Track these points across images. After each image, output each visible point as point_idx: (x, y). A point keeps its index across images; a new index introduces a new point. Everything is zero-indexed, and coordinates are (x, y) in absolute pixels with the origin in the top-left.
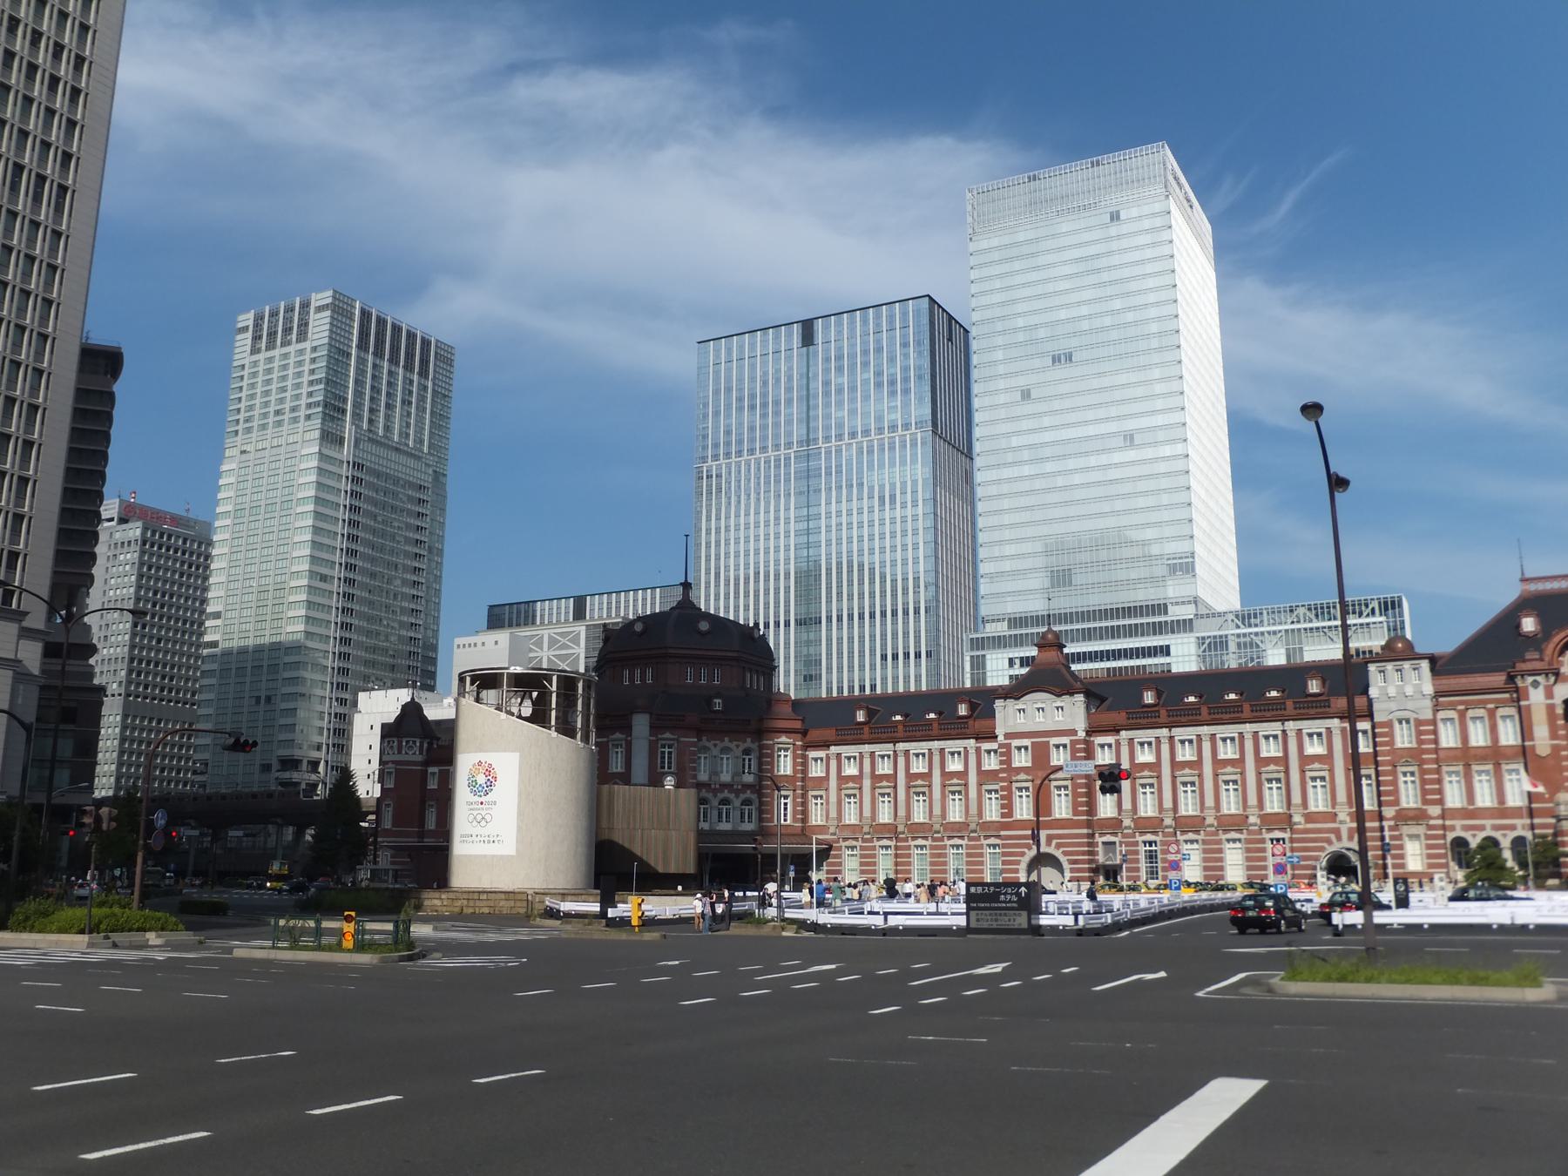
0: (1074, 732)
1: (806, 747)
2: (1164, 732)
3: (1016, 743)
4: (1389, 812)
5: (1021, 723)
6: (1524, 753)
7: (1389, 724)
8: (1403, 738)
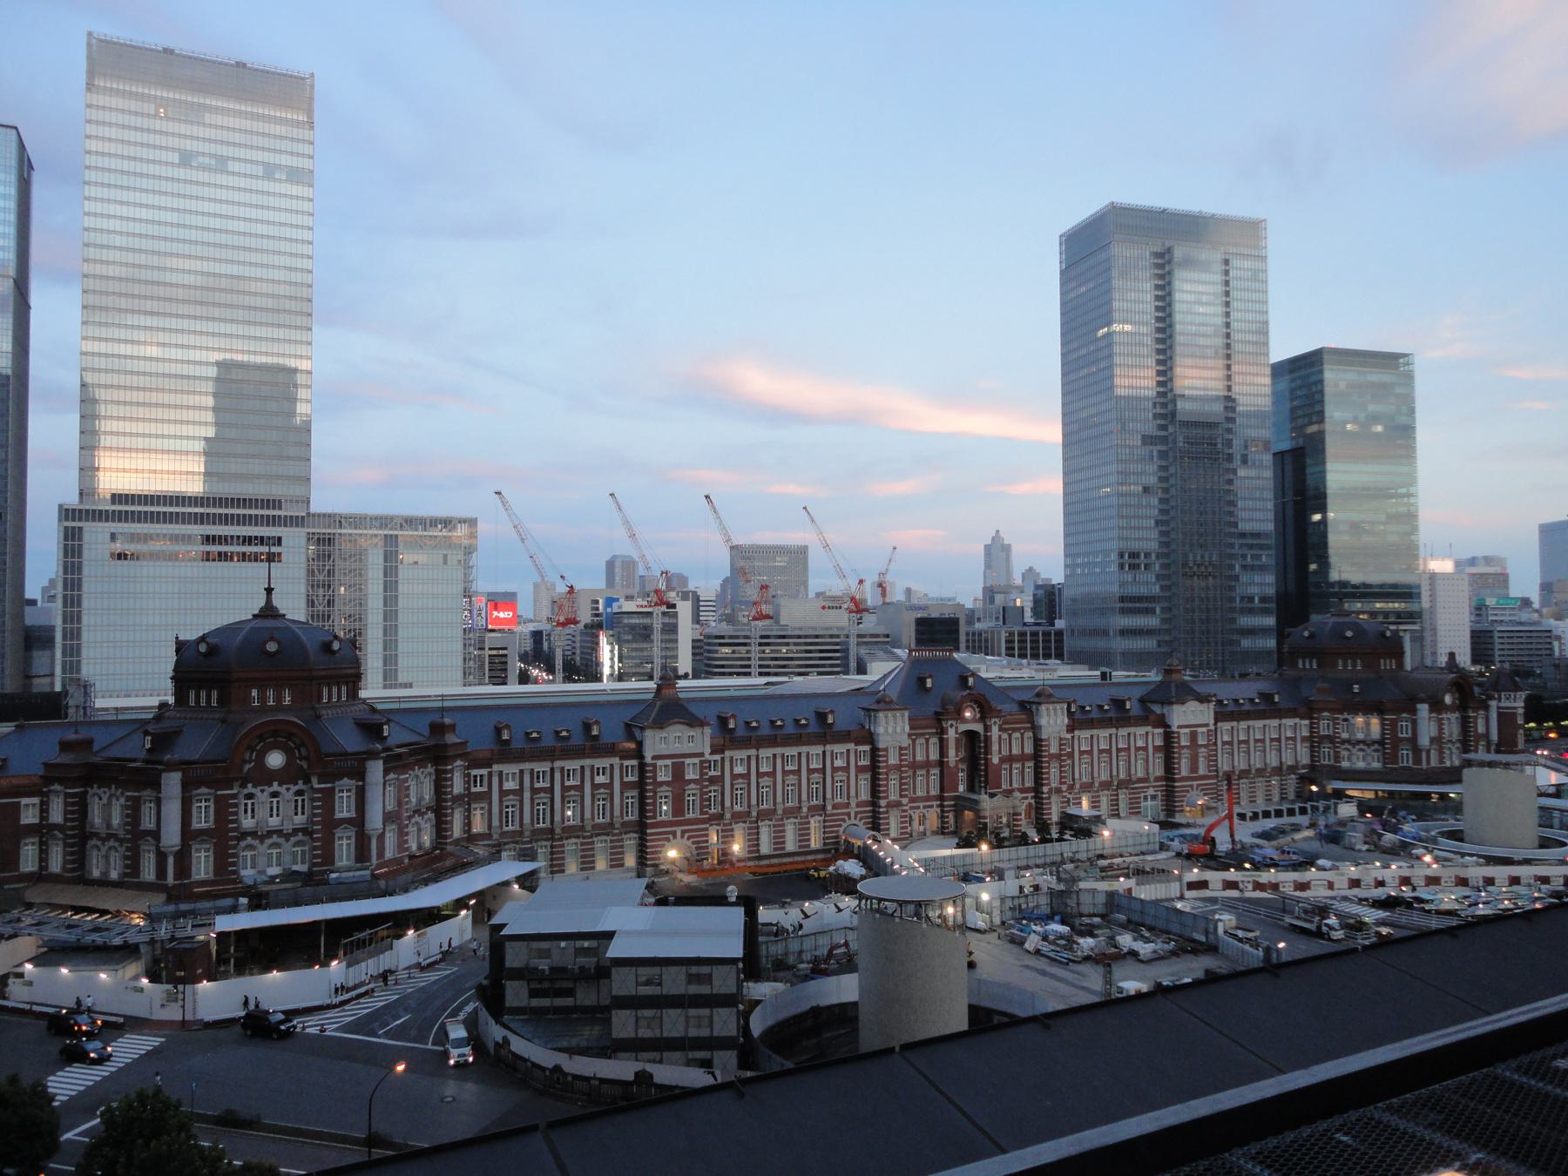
0: (702, 755)
1: (468, 768)
2: (753, 752)
3: (660, 763)
4: (883, 803)
5: (664, 749)
6: (941, 764)
7: (886, 750)
8: (893, 760)
